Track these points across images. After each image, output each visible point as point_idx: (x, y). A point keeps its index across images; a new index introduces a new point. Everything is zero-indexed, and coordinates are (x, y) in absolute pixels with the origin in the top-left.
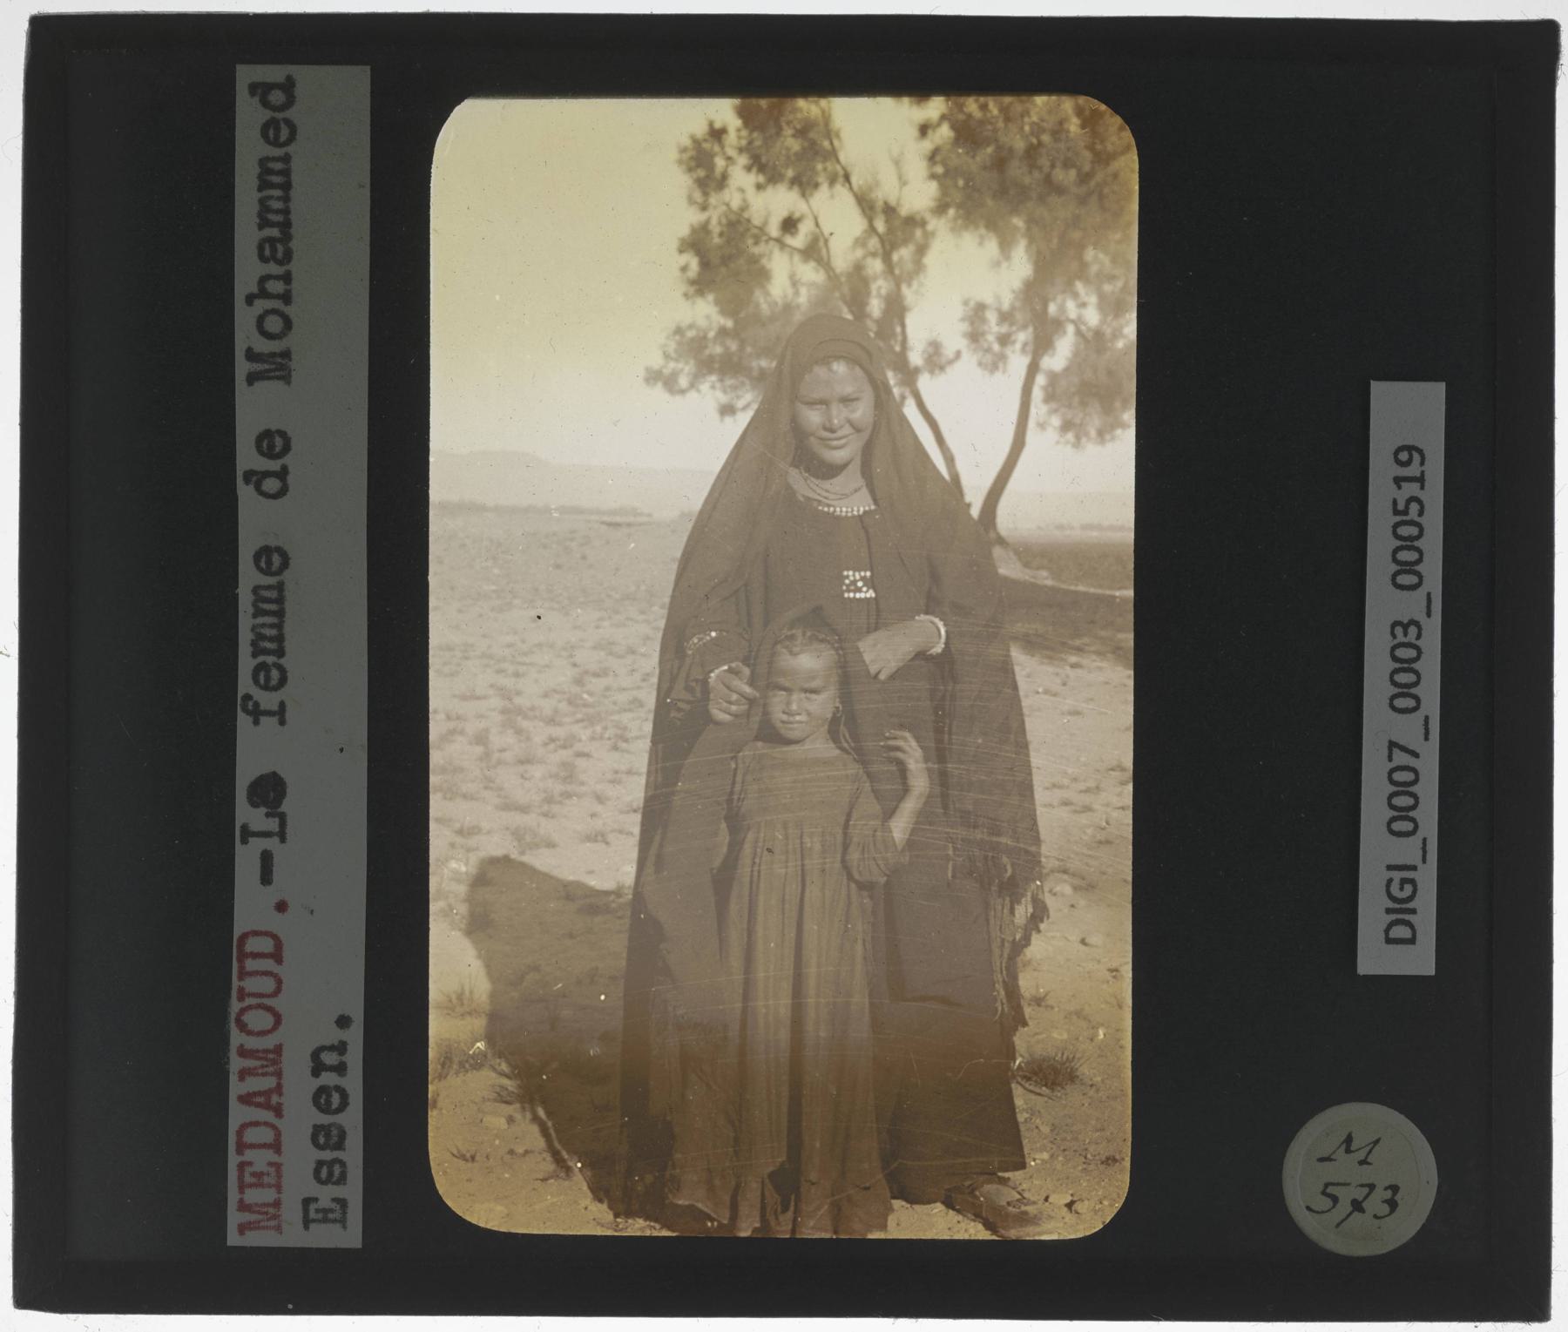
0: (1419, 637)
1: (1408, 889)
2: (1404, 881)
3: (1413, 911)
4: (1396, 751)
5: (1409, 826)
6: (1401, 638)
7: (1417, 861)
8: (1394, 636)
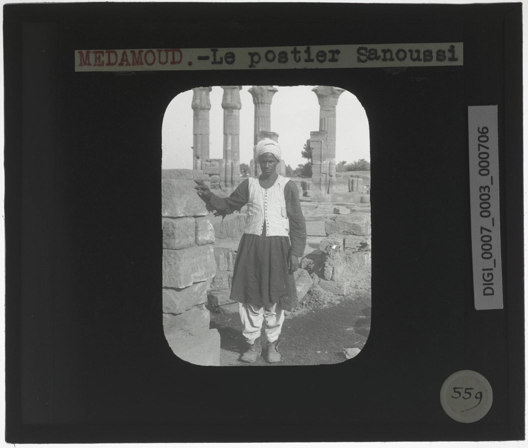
0: (489, 191)
1: (490, 277)
2: (488, 274)
3: (492, 284)
4: (483, 230)
5: (489, 255)
6: (483, 192)
7: (492, 266)
8: (481, 192)
